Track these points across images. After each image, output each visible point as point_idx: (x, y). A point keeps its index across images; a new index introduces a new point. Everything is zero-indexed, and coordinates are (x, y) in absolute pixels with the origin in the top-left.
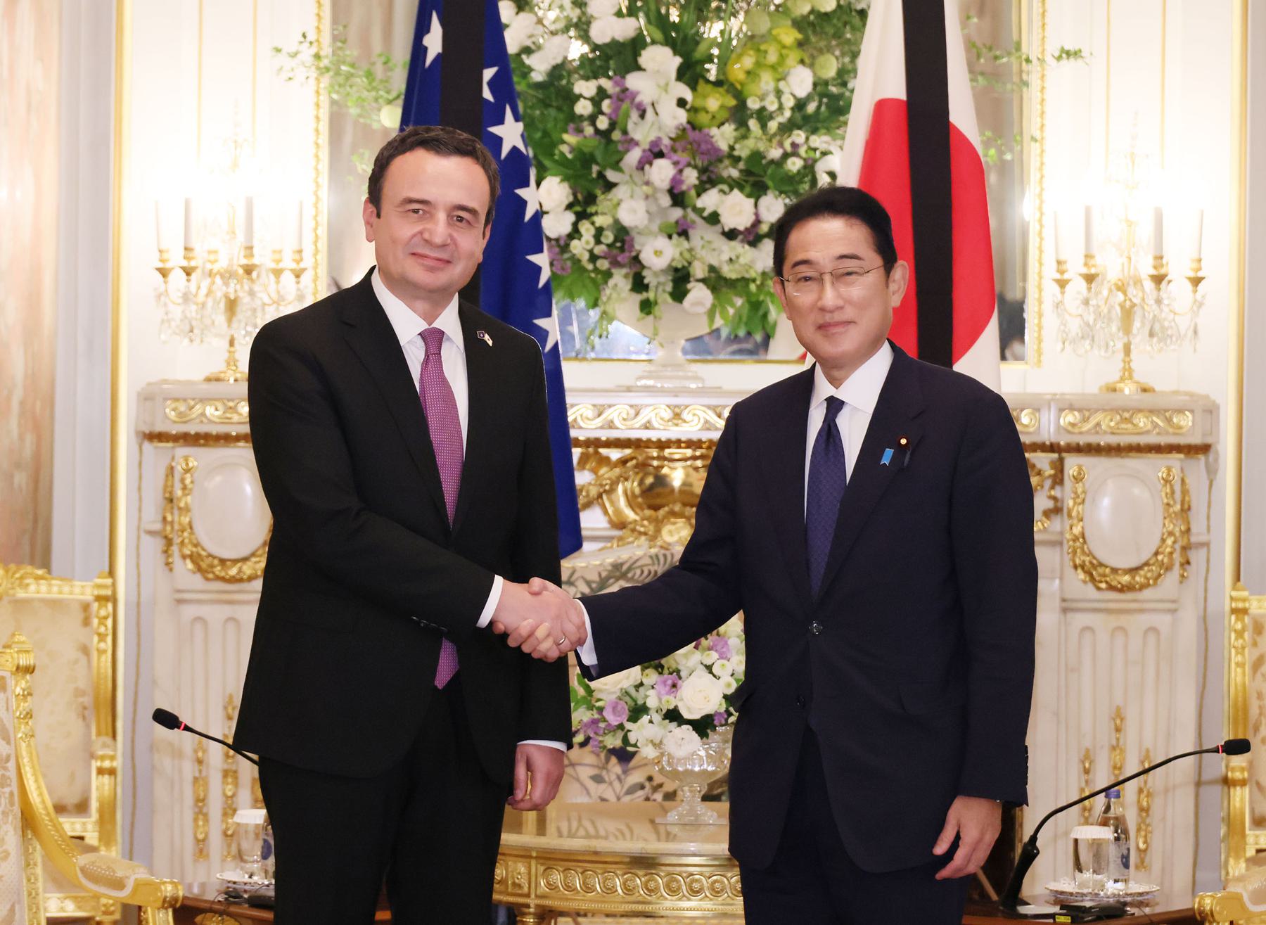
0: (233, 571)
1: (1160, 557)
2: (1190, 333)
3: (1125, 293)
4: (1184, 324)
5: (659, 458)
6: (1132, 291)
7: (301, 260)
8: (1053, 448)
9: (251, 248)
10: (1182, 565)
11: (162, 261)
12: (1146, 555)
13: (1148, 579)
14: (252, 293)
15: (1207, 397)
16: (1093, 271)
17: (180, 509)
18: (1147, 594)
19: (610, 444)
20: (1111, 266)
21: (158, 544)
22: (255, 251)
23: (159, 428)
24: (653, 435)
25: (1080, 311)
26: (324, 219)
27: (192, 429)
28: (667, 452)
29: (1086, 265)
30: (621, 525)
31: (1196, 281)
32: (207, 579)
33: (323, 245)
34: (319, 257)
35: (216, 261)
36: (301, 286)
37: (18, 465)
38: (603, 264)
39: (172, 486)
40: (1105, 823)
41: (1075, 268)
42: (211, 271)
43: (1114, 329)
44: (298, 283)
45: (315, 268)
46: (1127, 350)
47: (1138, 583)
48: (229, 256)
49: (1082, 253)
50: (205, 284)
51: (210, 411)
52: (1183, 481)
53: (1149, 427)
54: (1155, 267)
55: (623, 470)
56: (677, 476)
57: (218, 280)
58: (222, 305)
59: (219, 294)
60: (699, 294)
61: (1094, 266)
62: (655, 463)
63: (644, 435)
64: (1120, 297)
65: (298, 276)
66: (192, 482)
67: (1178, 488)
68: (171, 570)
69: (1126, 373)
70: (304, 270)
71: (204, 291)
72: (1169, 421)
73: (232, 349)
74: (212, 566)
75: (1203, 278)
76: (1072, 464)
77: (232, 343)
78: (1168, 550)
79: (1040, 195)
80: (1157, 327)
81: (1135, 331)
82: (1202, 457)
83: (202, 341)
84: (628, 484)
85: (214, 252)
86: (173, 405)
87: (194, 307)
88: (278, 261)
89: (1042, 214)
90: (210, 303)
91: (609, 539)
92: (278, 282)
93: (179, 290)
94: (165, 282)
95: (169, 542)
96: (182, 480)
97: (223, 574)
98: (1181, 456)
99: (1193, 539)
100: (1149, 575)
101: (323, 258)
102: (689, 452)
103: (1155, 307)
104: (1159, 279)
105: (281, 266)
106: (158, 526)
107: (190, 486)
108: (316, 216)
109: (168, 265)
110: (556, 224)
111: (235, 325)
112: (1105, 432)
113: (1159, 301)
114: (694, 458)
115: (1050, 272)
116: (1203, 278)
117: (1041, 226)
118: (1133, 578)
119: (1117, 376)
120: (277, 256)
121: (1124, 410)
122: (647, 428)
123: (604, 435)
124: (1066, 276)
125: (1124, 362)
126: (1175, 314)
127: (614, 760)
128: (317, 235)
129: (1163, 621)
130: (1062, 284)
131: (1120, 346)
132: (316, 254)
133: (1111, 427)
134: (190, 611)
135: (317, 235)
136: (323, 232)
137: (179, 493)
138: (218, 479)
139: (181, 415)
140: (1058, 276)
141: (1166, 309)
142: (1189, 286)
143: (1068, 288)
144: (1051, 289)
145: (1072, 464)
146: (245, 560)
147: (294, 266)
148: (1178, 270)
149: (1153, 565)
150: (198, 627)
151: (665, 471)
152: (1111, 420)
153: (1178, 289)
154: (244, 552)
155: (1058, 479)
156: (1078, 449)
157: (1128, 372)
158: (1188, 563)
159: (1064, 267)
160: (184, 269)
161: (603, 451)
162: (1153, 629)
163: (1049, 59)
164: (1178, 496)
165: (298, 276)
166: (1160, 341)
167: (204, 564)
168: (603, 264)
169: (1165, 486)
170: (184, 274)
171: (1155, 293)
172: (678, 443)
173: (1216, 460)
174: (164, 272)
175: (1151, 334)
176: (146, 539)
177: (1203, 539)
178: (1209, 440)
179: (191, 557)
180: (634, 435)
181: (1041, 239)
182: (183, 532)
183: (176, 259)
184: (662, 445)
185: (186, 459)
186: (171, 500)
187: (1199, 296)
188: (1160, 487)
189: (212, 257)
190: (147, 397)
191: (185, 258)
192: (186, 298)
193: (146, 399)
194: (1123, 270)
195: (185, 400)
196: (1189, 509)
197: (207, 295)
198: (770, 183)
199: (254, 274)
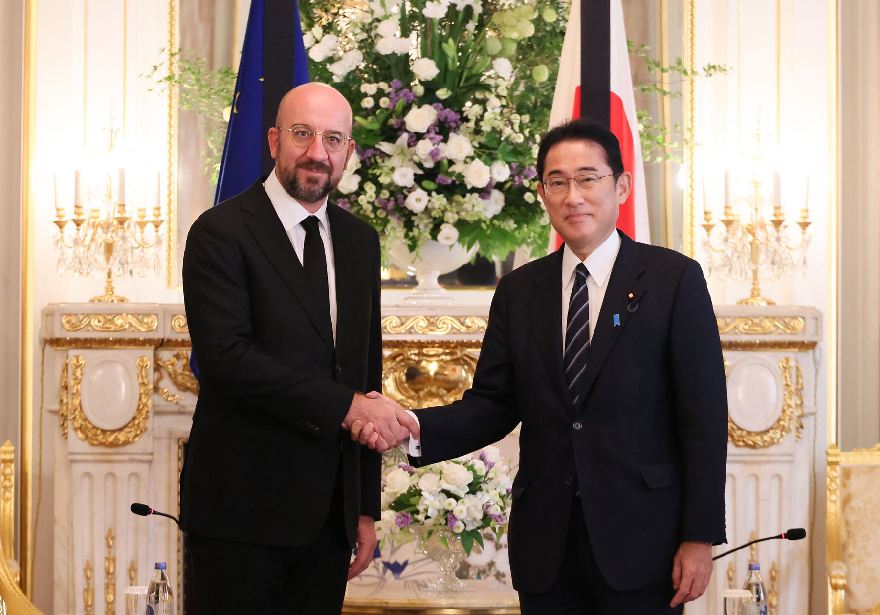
0: (111, 439)
1: (782, 423)
2: (801, 262)
3: (754, 235)
4: (796, 256)
5: (418, 355)
6: (760, 234)
7: (159, 215)
9: (124, 206)
10: (797, 429)
11: (59, 216)
12: (771, 423)
13: (773, 439)
14: (124, 238)
15: (814, 308)
16: (730, 218)
17: (74, 394)
18: (772, 449)
20: (744, 216)
21: (57, 420)
22: (126, 208)
23: (58, 334)
24: (415, 338)
25: (722, 247)
26: (174, 188)
27: (81, 335)
28: (425, 351)
29: (726, 213)
31: (804, 225)
32: (92, 445)
33: (174, 206)
34: (171, 216)
35: (98, 217)
36: (160, 233)
39: (67, 377)
41: (717, 216)
42: (94, 223)
43: (746, 261)
44: (157, 231)
45: (169, 222)
46: (755, 272)
47: (765, 441)
48: (107, 212)
49: (723, 205)
50: (90, 232)
51: (95, 322)
52: (797, 368)
53: (773, 329)
54: (775, 215)
55: (394, 364)
56: (432, 367)
57: (99, 230)
58: (102, 249)
59: (100, 241)
61: (732, 215)
62: (416, 358)
63: (409, 338)
64: (750, 237)
65: (157, 227)
66: (82, 374)
67: (794, 373)
68: (66, 438)
69: (756, 293)
70: (162, 222)
71: (89, 238)
72: (786, 325)
73: (110, 280)
74: (96, 435)
75: (809, 223)
77: (109, 275)
78: (787, 418)
79: (691, 167)
80: (777, 258)
81: (760, 261)
82: (811, 351)
83: (88, 273)
84: (396, 373)
85: (97, 211)
86: (68, 319)
87: (81, 249)
88: (143, 217)
89: (692, 180)
90: (93, 247)
92: (142, 232)
93: (71, 236)
94: (61, 232)
95: (65, 417)
96: (74, 374)
97: (103, 441)
98: (796, 350)
99: (806, 410)
100: (773, 436)
101: (174, 216)
102: (441, 350)
103: (776, 243)
104: (777, 223)
105: (145, 220)
106: (56, 407)
107: (80, 377)
108: (170, 185)
109: (63, 219)
111: (112, 261)
112: (741, 333)
113: (778, 239)
114: (446, 354)
115: (700, 219)
116: (809, 223)
117: (692, 189)
118: (762, 438)
119: (747, 294)
120: (141, 213)
121: (754, 317)
122: (411, 333)
124: (711, 223)
125: (754, 284)
126: (790, 249)
127: (389, 572)
128: (170, 200)
129: (783, 469)
130: (708, 228)
131: (750, 274)
132: (170, 212)
133: (745, 329)
134: (79, 469)
135: (170, 200)
136: (174, 197)
137: (71, 382)
138: (99, 372)
139: (73, 326)
140: (705, 223)
141: (783, 245)
142: (799, 228)
143: (713, 231)
144: (700, 232)
146: (121, 430)
147: (154, 219)
148: (791, 219)
149: (777, 429)
150: (86, 480)
151: (424, 363)
152: (746, 324)
153: (792, 232)
154: (120, 425)
157: (755, 293)
158: (802, 427)
159: (709, 216)
160: (75, 221)
162: (779, 477)
163: (698, 68)
164: (794, 379)
165: (157, 227)
166: (779, 268)
167: (90, 433)
169: (784, 371)
170: (75, 225)
171: (776, 233)
172: (432, 344)
173: (820, 355)
174: (60, 225)
175: (773, 263)
176: (47, 416)
177: (812, 410)
178: (814, 339)
179: (80, 428)
181: (692, 198)
182: (75, 411)
183: (69, 215)
184: (420, 345)
185: (77, 357)
186: (66, 388)
187: (807, 237)
188: (780, 372)
189: (95, 214)
190: (48, 314)
191: (76, 213)
192: (76, 242)
193: (47, 315)
194: (752, 219)
195: (76, 315)
196: (802, 388)
197: (93, 240)
198: (500, 156)
199: (126, 225)
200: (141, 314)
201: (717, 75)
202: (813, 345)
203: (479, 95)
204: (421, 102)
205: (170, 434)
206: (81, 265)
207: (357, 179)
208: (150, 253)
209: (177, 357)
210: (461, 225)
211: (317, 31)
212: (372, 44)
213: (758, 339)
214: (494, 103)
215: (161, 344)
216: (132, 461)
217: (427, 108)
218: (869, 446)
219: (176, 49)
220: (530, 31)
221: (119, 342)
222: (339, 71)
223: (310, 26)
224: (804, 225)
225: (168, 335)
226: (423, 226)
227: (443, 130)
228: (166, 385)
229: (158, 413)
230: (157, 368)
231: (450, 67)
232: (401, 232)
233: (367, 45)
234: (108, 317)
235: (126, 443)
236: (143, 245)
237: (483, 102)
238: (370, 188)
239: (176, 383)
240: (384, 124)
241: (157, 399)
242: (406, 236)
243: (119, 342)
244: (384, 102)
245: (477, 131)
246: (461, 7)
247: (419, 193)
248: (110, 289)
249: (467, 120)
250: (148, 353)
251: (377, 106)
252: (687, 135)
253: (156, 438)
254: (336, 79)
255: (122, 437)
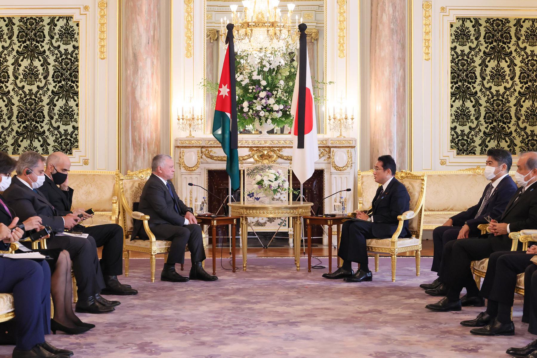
0: (191, 169)
4: (350, 126)
6: (342, 121)
8: (328, 147)
14: (194, 123)
18: (345, 171)
19: (254, 147)
21: (178, 165)
23: (179, 145)
26: (205, 111)
30: (256, 161)
31: (352, 119)
37: (154, 153)
38: (254, 117)
40: (340, 202)
41: (332, 117)
46: (341, 130)
48: (189, 116)
50: (186, 121)
51: (187, 142)
56: (266, 152)
60: (269, 121)
63: (260, 146)
67: (350, 153)
76: (332, 149)
91: (254, 163)
95: (180, 164)
101: (205, 117)
104: (346, 119)
106: (178, 162)
110: (246, 110)
113: (346, 122)
115: (328, 118)
116: (353, 119)
123: (253, 146)
130: (330, 120)
134: (183, 176)
137: (182, 156)
144: (328, 121)
145: (332, 149)
148: (349, 117)
153: (349, 121)
155: (330, 152)
156: (333, 147)
161: (253, 148)
168: (254, 117)
172: (265, 147)
174: (179, 120)
180: (258, 146)
183: (181, 117)
184: (263, 147)
190: (176, 140)
192: (183, 123)
200: (198, 140)
201: (332, 84)
202: (354, 147)
203: (276, 89)
204: (263, 90)
205: (205, 168)
206: (184, 129)
207: (248, 108)
208: (200, 126)
209: (206, 150)
210: (272, 119)
211: (238, 74)
212: (251, 77)
213: (342, 145)
214: (280, 91)
215: (203, 147)
216: (196, 174)
217: (264, 92)
218: (367, 170)
219: (205, 79)
220: (288, 74)
221: (193, 147)
222: (244, 83)
223: (237, 73)
224: (352, 119)
225: (204, 145)
226: (263, 120)
227: (268, 97)
228: (204, 156)
229: (202, 163)
230: (202, 152)
231: (270, 82)
232: (258, 121)
233: (250, 77)
234: (190, 141)
235: (195, 170)
236: (198, 124)
237: (277, 91)
238: (251, 111)
239: (206, 156)
240: (254, 96)
241: (202, 160)
242: (259, 122)
243: (193, 147)
244: (254, 91)
245: (276, 97)
246: (272, 68)
247: (262, 112)
248: (191, 135)
249: (274, 95)
250: (200, 149)
251: (252, 91)
252: (325, 98)
253: (201, 169)
254: (243, 85)
255: (193, 169)
